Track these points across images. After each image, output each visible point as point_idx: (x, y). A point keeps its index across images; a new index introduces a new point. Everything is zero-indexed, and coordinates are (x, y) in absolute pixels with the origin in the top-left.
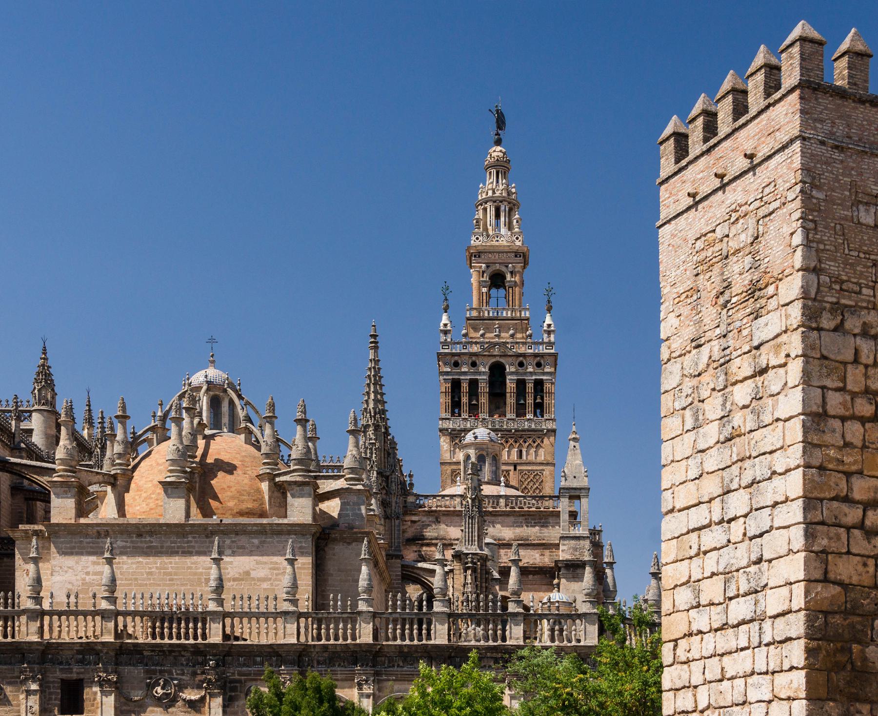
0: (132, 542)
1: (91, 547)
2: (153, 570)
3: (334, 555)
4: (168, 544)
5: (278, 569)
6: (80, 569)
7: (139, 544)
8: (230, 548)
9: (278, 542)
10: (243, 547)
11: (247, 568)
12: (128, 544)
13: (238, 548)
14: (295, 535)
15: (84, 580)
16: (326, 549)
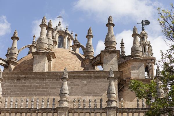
0: (14, 83)
4: (35, 84)
7: (18, 84)
9: (98, 82)
10: (77, 85)
12: (12, 85)
13: (75, 85)
16: (123, 90)
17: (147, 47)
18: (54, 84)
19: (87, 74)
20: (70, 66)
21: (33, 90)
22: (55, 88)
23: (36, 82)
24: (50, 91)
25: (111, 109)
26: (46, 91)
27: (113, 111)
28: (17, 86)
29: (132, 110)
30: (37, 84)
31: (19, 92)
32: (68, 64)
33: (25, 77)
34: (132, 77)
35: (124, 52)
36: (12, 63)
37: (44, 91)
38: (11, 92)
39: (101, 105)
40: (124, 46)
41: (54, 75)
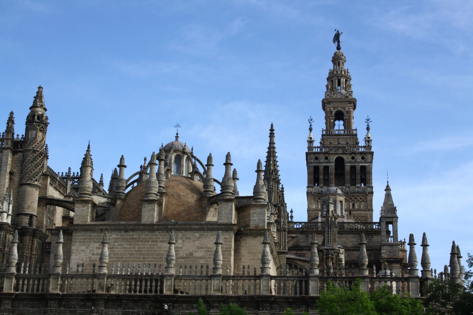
0: (121, 235)
2: (133, 252)
3: (246, 244)
4: (143, 236)
5: (211, 251)
6: (88, 251)
7: (125, 237)
8: (181, 238)
9: (211, 235)
10: (189, 238)
11: (192, 250)
12: (119, 237)
13: (186, 238)
14: (222, 230)
15: (90, 258)
16: (241, 240)
17: (343, 80)
19: (199, 226)
21: (142, 243)
23: (145, 235)
24: (159, 244)
25: (216, 277)
26: (156, 245)
27: (218, 279)
28: (125, 239)
29: (238, 278)
30: (146, 237)
31: (127, 245)
33: (133, 229)
34: (251, 224)
35: (274, 143)
37: (154, 245)
38: (118, 245)
39: (207, 272)
40: (274, 134)
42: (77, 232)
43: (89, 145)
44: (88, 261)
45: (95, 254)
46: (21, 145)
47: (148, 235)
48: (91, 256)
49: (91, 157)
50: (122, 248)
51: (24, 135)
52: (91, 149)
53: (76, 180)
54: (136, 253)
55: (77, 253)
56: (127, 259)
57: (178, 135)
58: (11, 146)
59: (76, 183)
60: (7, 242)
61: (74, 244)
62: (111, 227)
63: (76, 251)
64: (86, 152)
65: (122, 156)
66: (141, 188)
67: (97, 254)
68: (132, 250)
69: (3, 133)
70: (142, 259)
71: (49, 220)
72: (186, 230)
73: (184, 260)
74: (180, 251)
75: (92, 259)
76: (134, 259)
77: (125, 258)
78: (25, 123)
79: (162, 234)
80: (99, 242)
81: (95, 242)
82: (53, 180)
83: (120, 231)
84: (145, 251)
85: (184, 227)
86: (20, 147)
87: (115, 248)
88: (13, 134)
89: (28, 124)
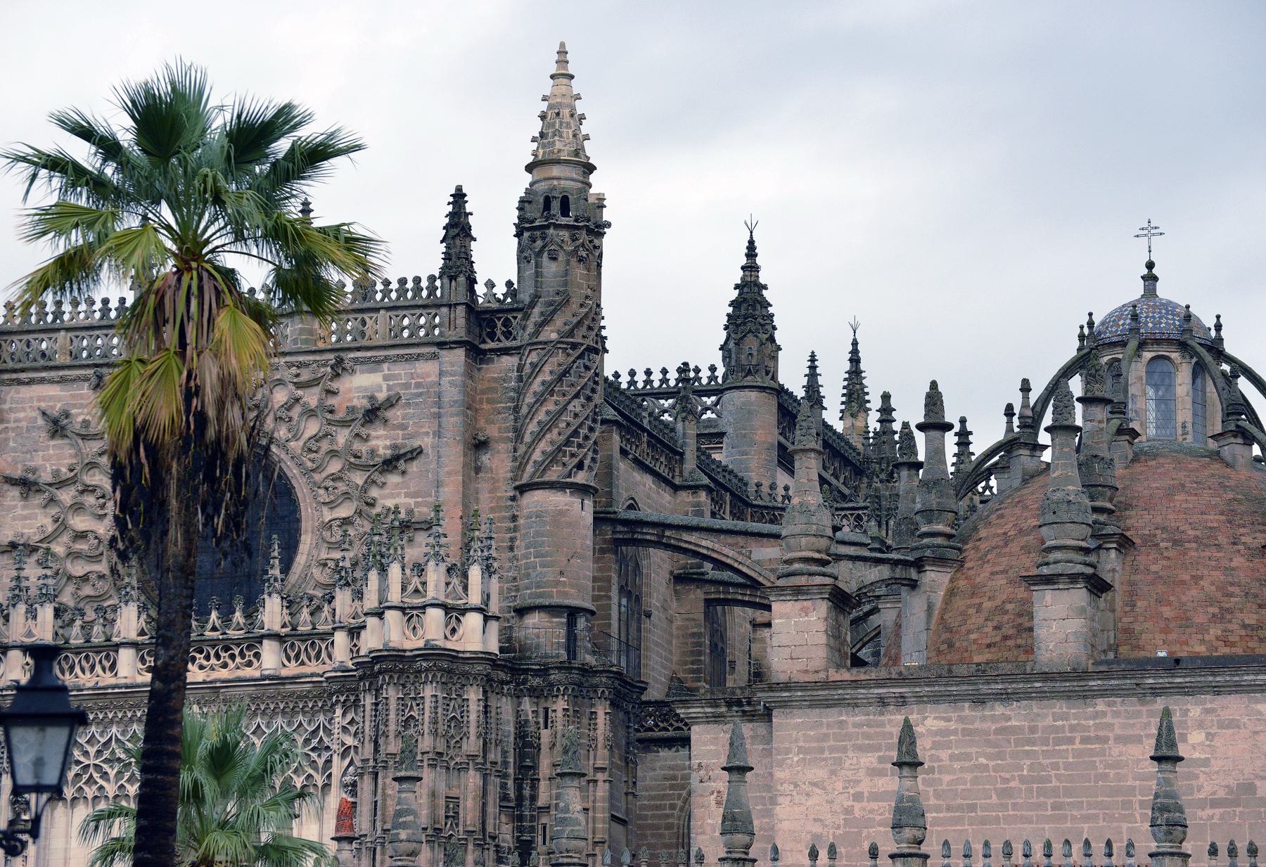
0: (961, 719)
1: (867, 736)
2: (1012, 784)
4: (1049, 721)
6: (839, 785)
7: (977, 725)
8: (1201, 725)
10: (1233, 724)
13: (1222, 725)
15: (848, 811)
18: (1131, 722)
20: (1202, 589)
21: (1045, 748)
22: (1138, 740)
26: (1102, 753)
30: (1057, 723)
32: (1193, 577)
33: (1007, 694)
36: (933, 565)
37: (1092, 753)
41: (1128, 681)
42: (788, 711)
43: (751, 242)
44: (842, 822)
45: (866, 794)
46: (507, 323)
47: (1065, 717)
48: (850, 803)
49: (764, 292)
50: (970, 770)
51: (515, 281)
52: (759, 261)
53: (709, 401)
54: (1023, 787)
55: (794, 793)
56: (994, 814)
57: (1154, 271)
58: (469, 332)
59: (709, 415)
60: (494, 726)
61: (784, 760)
62: (918, 689)
63: (792, 787)
64: (741, 273)
65: (934, 385)
66: (1017, 511)
67: (875, 797)
68: (1007, 776)
69: (432, 279)
70: (1049, 813)
71: (624, 601)
72: (1217, 690)
73: (1222, 810)
74: (1202, 778)
75: (857, 813)
76: (1018, 813)
77: (984, 809)
78: (513, 230)
79: (1122, 709)
80: (876, 748)
81: (860, 748)
82: (629, 431)
83: (955, 701)
84: (1058, 777)
85: (1210, 678)
86: (503, 333)
87: (940, 772)
88: (472, 281)
89: (526, 234)
